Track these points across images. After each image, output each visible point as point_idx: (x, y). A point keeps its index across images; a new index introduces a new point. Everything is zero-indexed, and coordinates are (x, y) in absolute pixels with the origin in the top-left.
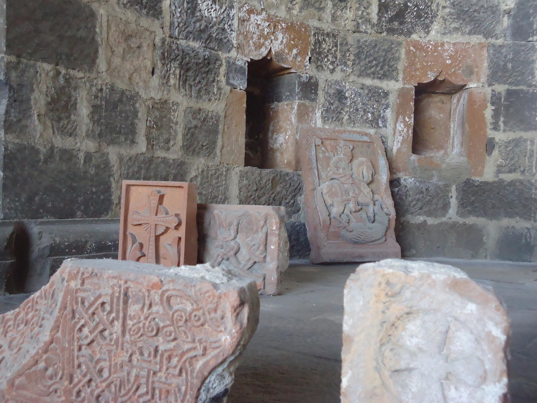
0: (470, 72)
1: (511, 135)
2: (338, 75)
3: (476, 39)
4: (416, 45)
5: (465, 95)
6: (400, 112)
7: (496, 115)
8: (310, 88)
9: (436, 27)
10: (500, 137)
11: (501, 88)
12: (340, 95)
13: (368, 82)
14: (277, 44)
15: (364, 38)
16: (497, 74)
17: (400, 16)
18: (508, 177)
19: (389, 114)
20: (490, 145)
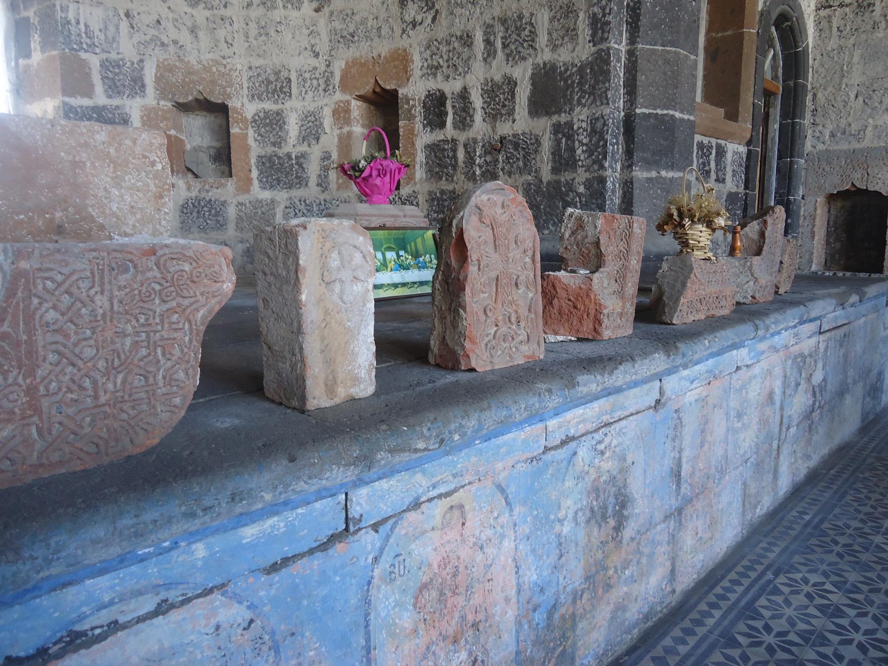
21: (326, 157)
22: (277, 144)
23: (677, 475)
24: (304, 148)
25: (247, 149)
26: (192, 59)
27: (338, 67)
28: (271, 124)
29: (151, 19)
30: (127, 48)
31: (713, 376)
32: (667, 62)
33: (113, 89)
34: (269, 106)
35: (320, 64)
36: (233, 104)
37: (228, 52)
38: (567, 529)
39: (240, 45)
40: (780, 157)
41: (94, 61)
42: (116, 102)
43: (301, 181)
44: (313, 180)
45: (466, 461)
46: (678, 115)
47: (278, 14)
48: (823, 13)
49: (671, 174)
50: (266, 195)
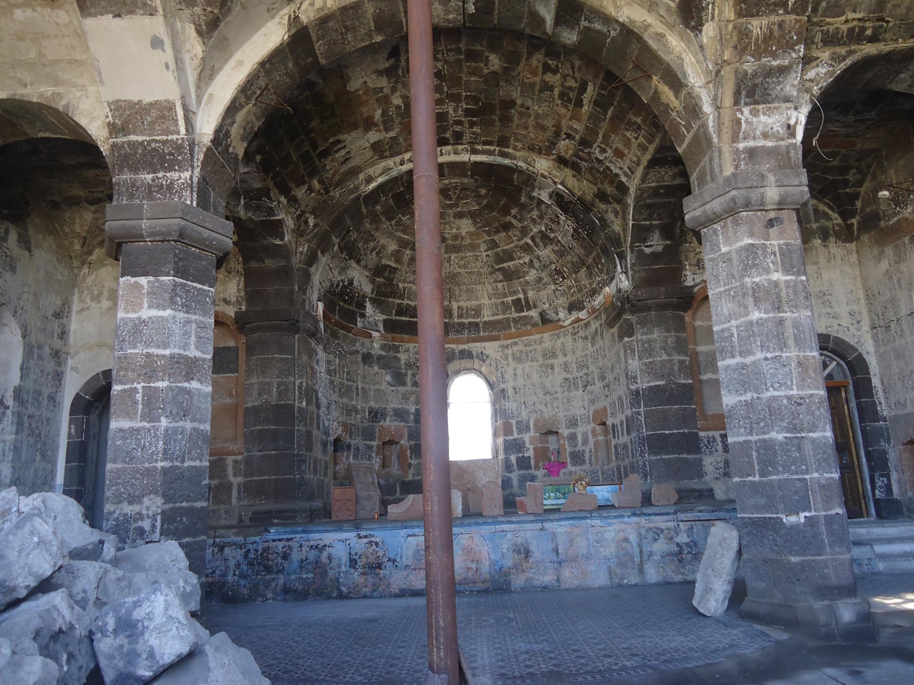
0: (401, 437)
1: (417, 461)
2: (357, 441)
3: (402, 424)
4: (382, 426)
5: (399, 446)
6: (378, 454)
7: (411, 454)
8: (349, 446)
9: (388, 419)
10: (413, 462)
11: (412, 443)
12: (358, 449)
13: (366, 442)
14: (339, 432)
15: (365, 425)
16: (411, 437)
17: (376, 416)
18: (417, 478)
19: (374, 455)
20: (410, 465)
21: (591, 451)
22: (575, 446)
23: (556, 551)
24: (584, 448)
25: (565, 449)
26: (546, 416)
27: (591, 412)
28: (573, 438)
29: (531, 403)
30: (524, 416)
31: (572, 526)
32: (658, 412)
33: (520, 431)
34: (572, 431)
35: (586, 412)
36: (560, 431)
37: (557, 411)
38: (505, 551)
39: (561, 408)
40: (860, 423)
41: (514, 422)
42: (521, 436)
43: (584, 462)
44: (588, 461)
45: (473, 529)
46: (667, 432)
47: (572, 394)
48: (875, 331)
49: (667, 457)
50: (573, 469)
